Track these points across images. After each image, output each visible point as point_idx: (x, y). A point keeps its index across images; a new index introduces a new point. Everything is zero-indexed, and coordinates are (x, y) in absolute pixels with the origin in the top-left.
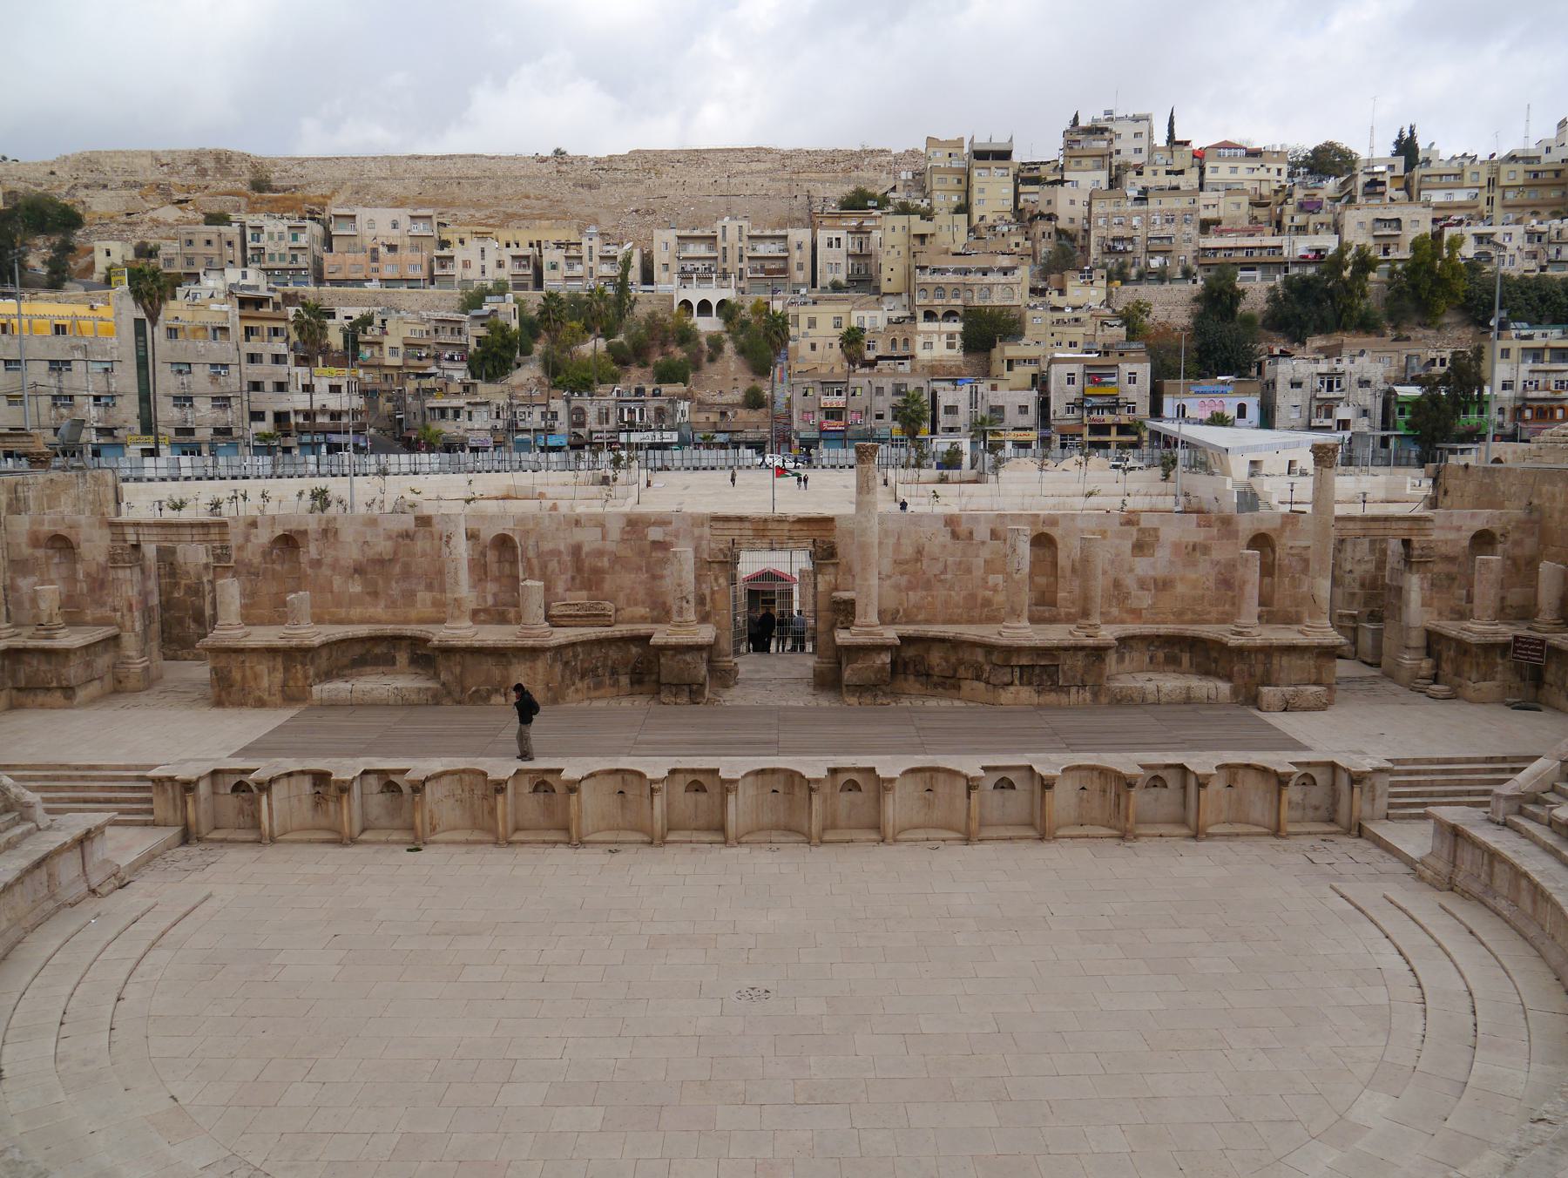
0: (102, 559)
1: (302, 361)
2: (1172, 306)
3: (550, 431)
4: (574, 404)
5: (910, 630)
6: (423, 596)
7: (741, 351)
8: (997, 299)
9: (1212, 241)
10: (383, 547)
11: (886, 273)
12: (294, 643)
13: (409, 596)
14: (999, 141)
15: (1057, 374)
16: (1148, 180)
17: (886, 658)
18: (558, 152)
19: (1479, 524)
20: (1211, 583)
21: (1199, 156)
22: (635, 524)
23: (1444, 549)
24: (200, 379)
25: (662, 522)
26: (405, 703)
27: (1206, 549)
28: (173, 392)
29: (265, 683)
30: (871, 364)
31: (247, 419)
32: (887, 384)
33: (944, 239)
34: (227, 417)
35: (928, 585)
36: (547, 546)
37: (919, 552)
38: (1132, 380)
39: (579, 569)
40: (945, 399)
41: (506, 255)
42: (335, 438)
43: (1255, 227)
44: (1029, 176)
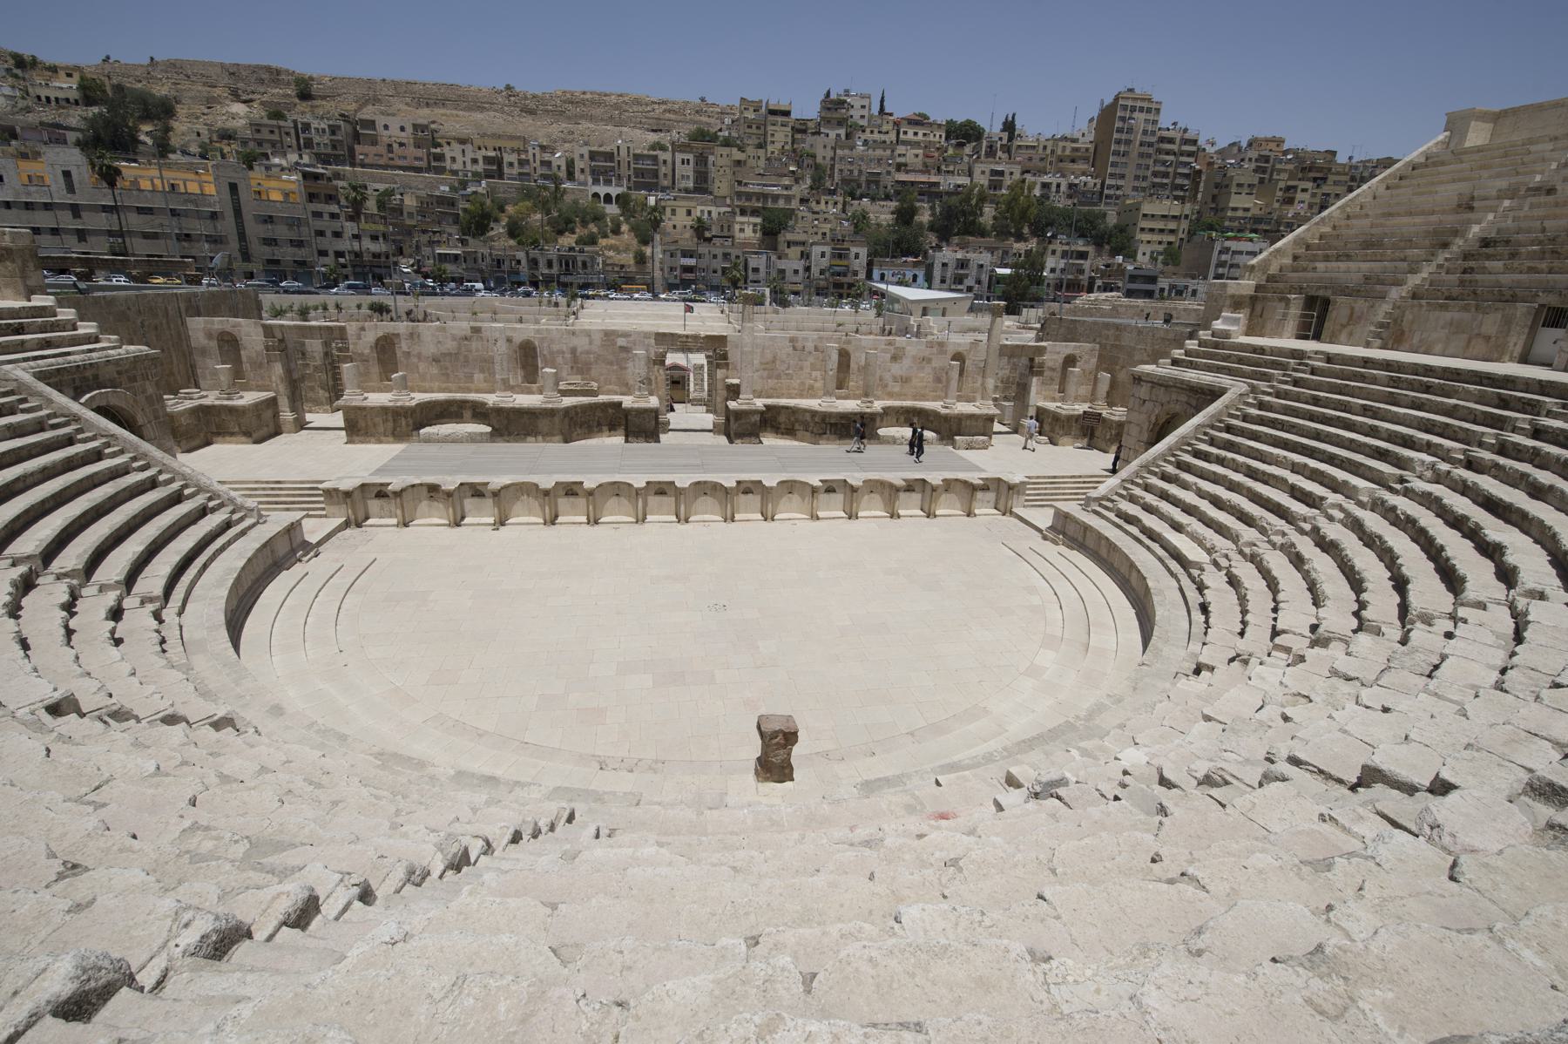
1: (351, 218)
2: (882, 214)
3: (518, 273)
5: (769, 401)
6: (478, 376)
7: (633, 229)
8: (781, 204)
9: (902, 177)
10: (450, 345)
11: (717, 184)
13: (470, 377)
14: (783, 106)
15: (816, 250)
16: (867, 135)
17: (757, 418)
18: (508, 87)
19: (1069, 351)
21: (897, 124)
22: (609, 335)
25: (626, 335)
26: (473, 439)
27: (929, 361)
30: (709, 240)
32: (719, 252)
33: (752, 162)
34: (301, 254)
35: (778, 377)
36: (555, 347)
38: (857, 256)
40: (752, 263)
41: (480, 155)
42: (377, 271)
43: (926, 170)
44: (801, 129)
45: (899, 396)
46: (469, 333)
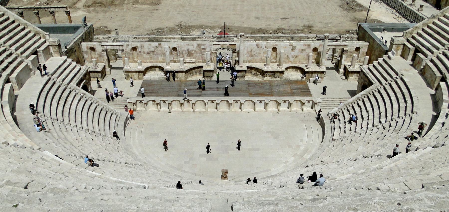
0: (101, 51)
5: (249, 65)
10: (153, 49)
12: (140, 70)
23: (350, 50)
29: (135, 76)
36: (183, 49)
37: (252, 50)
39: (189, 52)
46: (157, 45)
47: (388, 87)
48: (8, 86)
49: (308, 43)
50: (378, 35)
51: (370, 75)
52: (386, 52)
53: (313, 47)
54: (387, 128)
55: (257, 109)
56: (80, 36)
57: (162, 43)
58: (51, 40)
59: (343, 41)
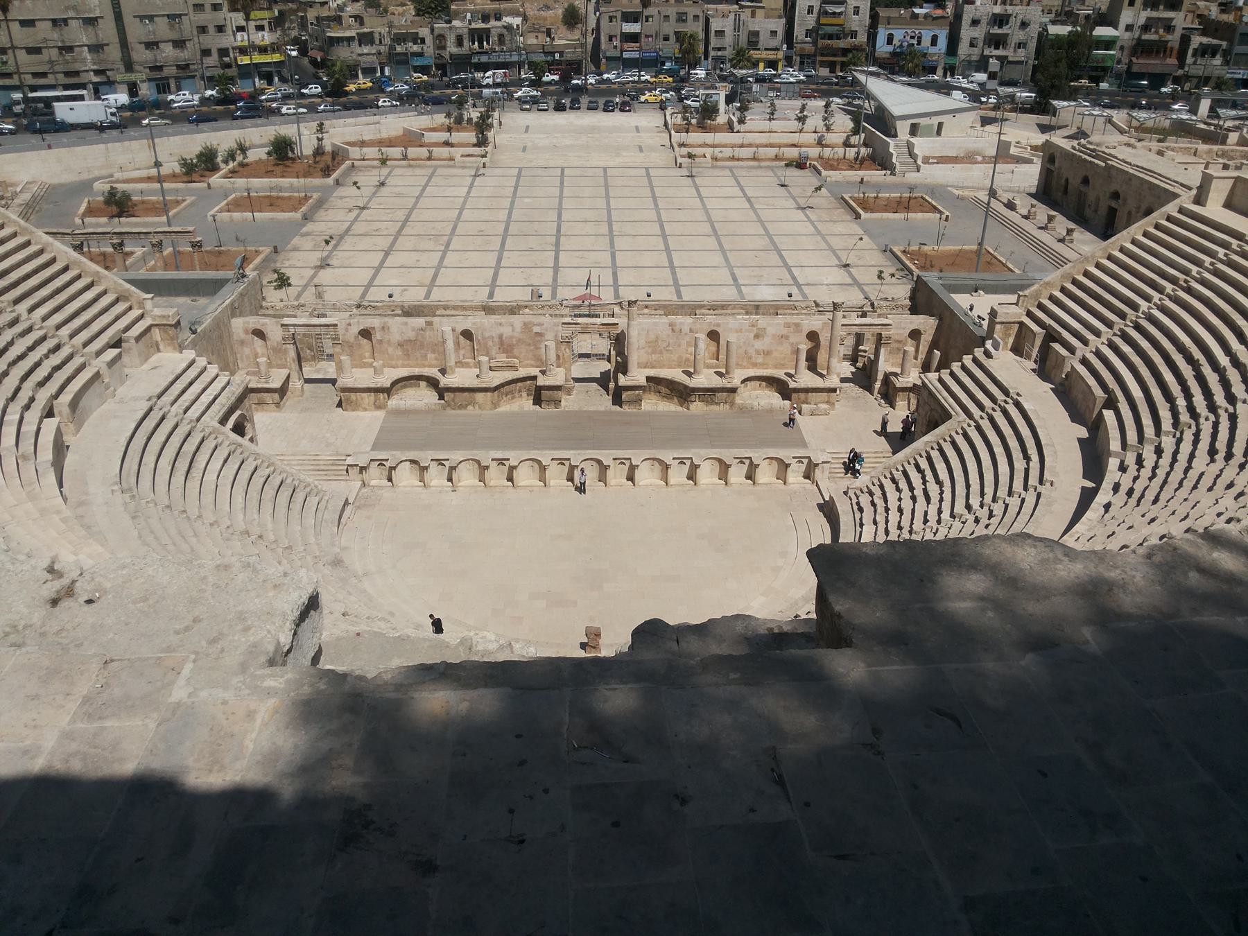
4: (437, 32)
5: (652, 372)
10: (411, 335)
13: (425, 357)
20: (789, 352)
23: (897, 338)
24: (162, 28)
27: (787, 338)
28: (144, 40)
29: (366, 401)
31: (199, 53)
35: (661, 352)
36: (487, 334)
39: (502, 343)
40: (715, 25)
45: (763, 365)
47: (985, 424)
48: (50, 425)
49: (796, 319)
50: (962, 300)
51: (943, 397)
52: (981, 342)
53: (806, 331)
54: (984, 521)
55: (672, 481)
56: (228, 302)
57: (436, 320)
58: (157, 312)
59: (880, 316)
